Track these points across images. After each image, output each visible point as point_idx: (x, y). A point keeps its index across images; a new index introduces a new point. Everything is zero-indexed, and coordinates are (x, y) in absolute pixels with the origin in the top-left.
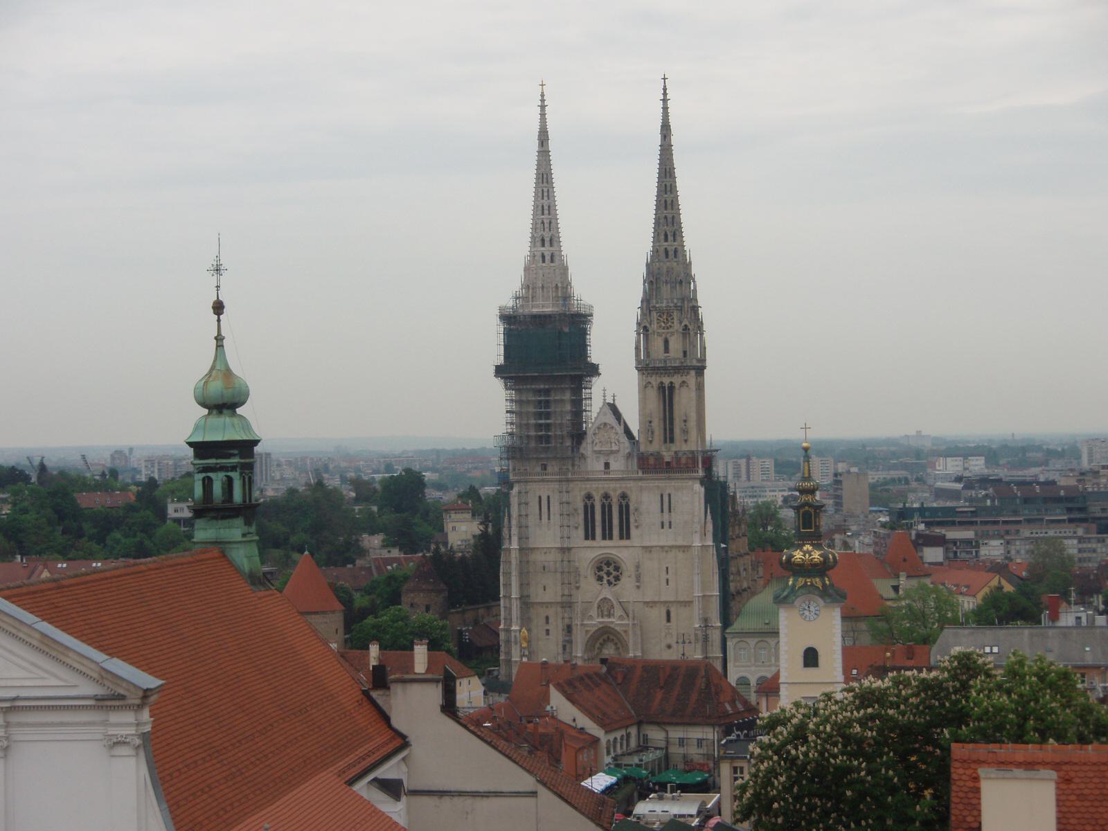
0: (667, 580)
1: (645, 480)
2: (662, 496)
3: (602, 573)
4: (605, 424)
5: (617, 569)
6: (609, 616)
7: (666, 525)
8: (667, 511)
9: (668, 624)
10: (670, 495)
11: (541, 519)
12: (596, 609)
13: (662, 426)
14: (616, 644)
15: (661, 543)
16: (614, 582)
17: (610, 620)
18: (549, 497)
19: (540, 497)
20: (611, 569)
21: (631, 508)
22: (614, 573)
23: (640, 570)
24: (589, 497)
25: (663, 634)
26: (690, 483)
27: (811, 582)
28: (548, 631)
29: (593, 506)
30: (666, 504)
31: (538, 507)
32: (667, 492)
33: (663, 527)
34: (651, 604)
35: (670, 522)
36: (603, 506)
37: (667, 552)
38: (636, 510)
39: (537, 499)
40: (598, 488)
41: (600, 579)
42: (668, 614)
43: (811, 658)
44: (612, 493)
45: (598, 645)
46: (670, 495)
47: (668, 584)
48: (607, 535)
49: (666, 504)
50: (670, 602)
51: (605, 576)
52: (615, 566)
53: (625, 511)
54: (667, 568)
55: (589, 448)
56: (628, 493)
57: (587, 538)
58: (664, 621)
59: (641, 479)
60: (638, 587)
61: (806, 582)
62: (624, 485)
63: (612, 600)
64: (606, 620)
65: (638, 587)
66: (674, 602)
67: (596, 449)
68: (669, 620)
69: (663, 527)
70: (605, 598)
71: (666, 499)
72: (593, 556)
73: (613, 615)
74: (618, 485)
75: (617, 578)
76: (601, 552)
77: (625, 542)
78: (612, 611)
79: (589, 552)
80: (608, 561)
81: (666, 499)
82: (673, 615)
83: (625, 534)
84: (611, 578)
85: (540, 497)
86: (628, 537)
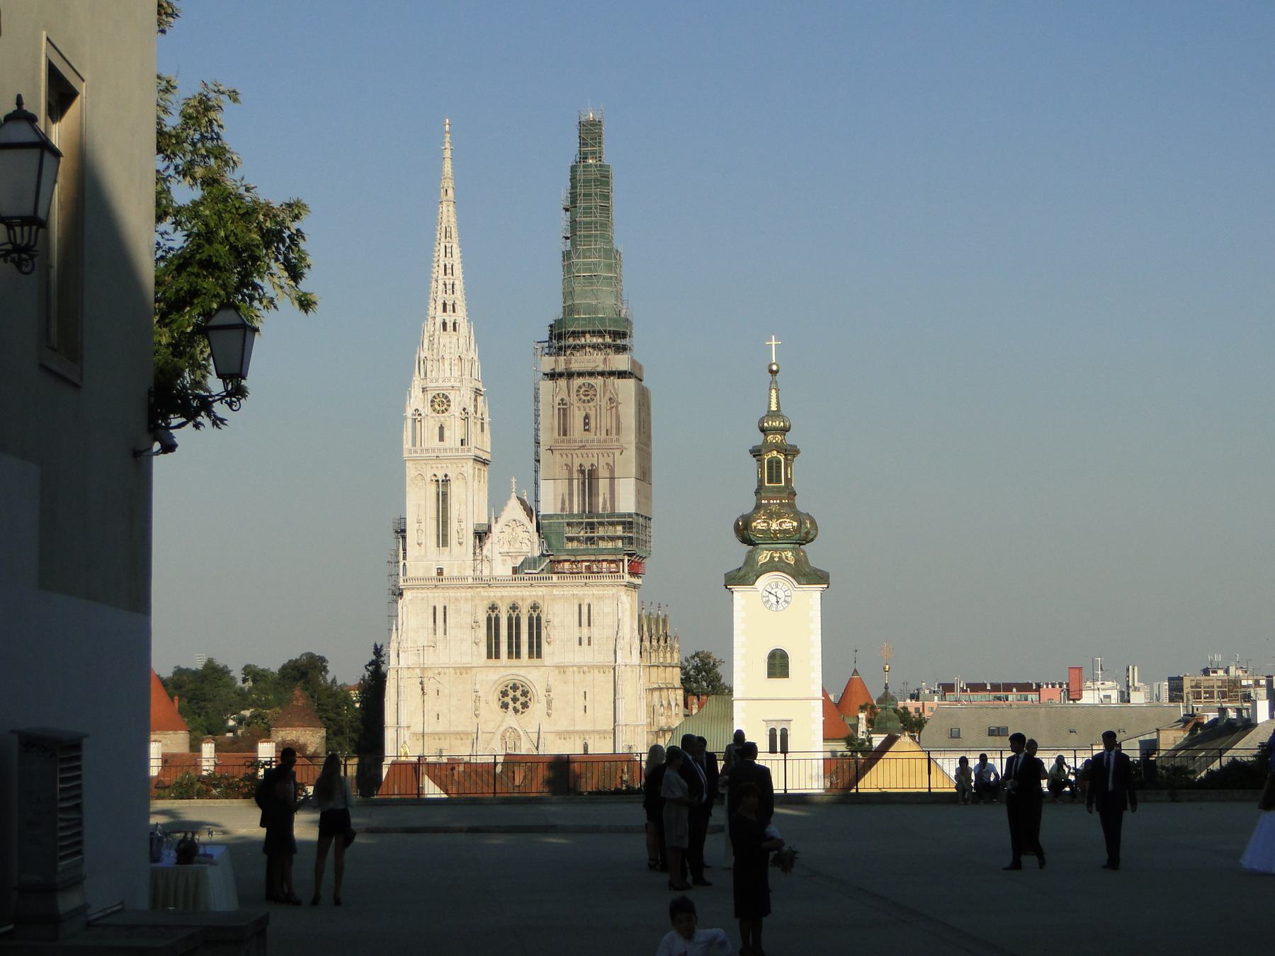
0: (585, 707)
2: (580, 606)
5: (525, 694)
7: (585, 641)
8: (587, 624)
10: (589, 605)
11: (435, 634)
16: (521, 710)
18: (445, 608)
19: (435, 608)
22: (522, 699)
24: (493, 608)
26: (614, 590)
27: (780, 558)
29: (497, 619)
30: (585, 616)
32: (586, 602)
33: (580, 644)
34: (564, 735)
35: (589, 638)
40: (502, 596)
41: (505, 706)
43: (778, 664)
44: (520, 603)
46: (589, 605)
49: (585, 616)
51: (511, 705)
53: (536, 625)
54: (585, 692)
55: (497, 548)
56: (541, 602)
57: (489, 656)
60: (549, 715)
61: (772, 557)
62: (534, 593)
66: (594, 732)
67: (501, 550)
69: (580, 644)
71: (585, 610)
72: (496, 677)
75: (525, 705)
76: (505, 674)
77: (535, 661)
78: (518, 744)
80: (515, 684)
81: (585, 610)
83: (536, 650)
84: (518, 705)
85: (435, 608)
86: (539, 655)
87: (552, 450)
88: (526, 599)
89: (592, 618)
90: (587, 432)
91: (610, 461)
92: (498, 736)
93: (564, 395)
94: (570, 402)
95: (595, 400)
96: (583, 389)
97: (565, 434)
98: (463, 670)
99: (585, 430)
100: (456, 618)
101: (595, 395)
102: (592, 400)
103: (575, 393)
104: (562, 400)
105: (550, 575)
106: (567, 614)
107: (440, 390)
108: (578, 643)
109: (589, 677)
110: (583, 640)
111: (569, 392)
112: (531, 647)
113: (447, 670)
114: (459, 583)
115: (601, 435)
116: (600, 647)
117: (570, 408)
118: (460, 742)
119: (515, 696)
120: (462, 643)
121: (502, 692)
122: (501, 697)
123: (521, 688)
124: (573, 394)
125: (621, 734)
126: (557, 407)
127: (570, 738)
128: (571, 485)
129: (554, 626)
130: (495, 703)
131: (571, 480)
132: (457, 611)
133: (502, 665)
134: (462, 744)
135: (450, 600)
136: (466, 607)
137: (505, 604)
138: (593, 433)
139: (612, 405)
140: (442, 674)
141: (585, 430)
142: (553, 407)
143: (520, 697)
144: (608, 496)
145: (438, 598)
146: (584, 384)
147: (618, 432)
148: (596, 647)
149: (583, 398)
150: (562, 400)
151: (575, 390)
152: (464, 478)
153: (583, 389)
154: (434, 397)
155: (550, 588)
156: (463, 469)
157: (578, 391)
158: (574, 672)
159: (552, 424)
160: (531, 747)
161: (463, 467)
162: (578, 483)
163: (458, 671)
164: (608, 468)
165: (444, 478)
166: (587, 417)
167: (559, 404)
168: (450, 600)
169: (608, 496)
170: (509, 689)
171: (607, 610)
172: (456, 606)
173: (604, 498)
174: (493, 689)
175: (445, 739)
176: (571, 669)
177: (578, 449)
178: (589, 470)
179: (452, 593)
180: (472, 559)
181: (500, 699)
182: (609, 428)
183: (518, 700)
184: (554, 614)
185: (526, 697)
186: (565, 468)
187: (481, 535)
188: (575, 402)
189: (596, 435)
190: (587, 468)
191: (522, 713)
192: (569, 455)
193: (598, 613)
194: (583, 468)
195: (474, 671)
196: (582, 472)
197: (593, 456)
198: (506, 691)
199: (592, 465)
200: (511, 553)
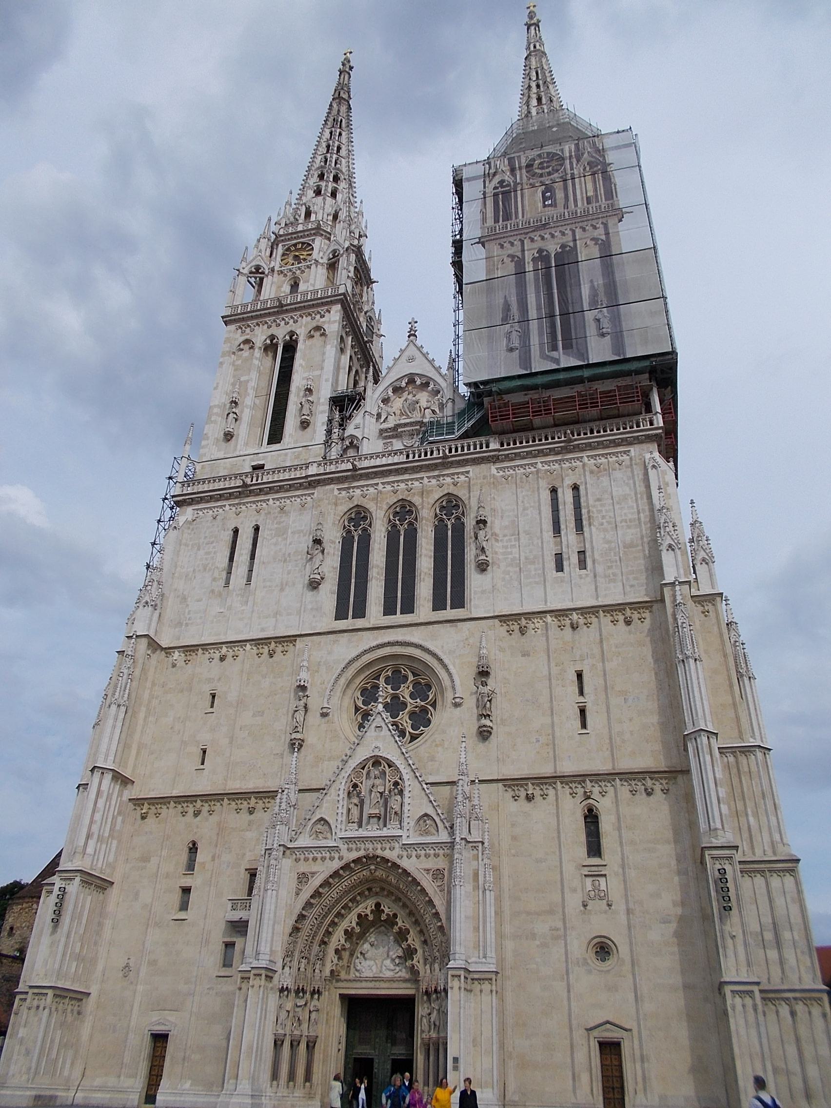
0: (583, 711)
1: (508, 458)
2: (554, 491)
4: (411, 380)
5: (422, 689)
6: (382, 819)
8: (572, 524)
9: (595, 861)
10: (576, 488)
12: (343, 795)
14: (402, 936)
17: (385, 832)
18: (257, 529)
19: (236, 531)
20: (405, 692)
21: (469, 522)
23: (490, 681)
26: (634, 450)
28: (186, 891)
31: (227, 554)
32: (568, 482)
33: (560, 567)
35: (582, 553)
37: (574, 627)
38: (482, 523)
39: (228, 535)
42: (591, 818)
44: (416, 500)
45: (338, 938)
46: (576, 488)
47: (584, 725)
50: (596, 777)
52: (416, 684)
54: (580, 675)
56: (462, 493)
57: (341, 614)
58: (582, 850)
59: (495, 459)
63: (399, 762)
64: (372, 830)
65: (484, 734)
66: (610, 776)
67: (385, 426)
68: (594, 848)
69: (560, 567)
70: (377, 761)
71: (566, 497)
73: (399, 815)
75: (421, 719)
76: (374, 644)
77: (449, 613)
81: (566, 497)
82: (606, 825)
84: (404, 719)
85: (236, 531)
86: (459, 602)
88: (430, 492)
89: (584, 511)
91: (600, 233)
92: (342, 785)
100: (276, 544)
102: (557, 171)
104: (502, 182)
105: (483, 439)
106: (524, 509)
107: (298, 238)
108: (551, 564)
109: (588, 636)
110: (565, 556)
111: (513, 170)
115: (576, 205)
116: (610, 567)
117: (515, 191)
118: (245, 816)
119: (395, 697)
120: (282, 590)
121: (364, 691)
122: (360, 704)
123: (411, 678)
125: (708, 758)
127: (544, 796)
128: (521, 286)
129: (494, 534)
130: (345, 716)
131: (520, 272)
134: (250, 823)
137: (385, 507)
138: (560, 209)
139: (595, 169)
140: (229, 659)
141: (545, 206)
142: (484, 194)
143: (409, 700)
144: (600, 281)
146: (539, 156)
148: (600, 569)
149: (540, 171)
151: (524, 164)
152: (323, 335)
154: (288, 249)
156: (322, 320)
157: (528, 166)
160: (430, 811)
161: (322, 316)
164: (596, 244)
165: (288, 338)
167: (495, 188)
169: (601, 282)
170: (382, 682)
171: (617, 491)
172: (279, 523)
173: (592, 288)
174: (343, 681)
175: (210, 812)
176: (538, 623)
177: (534, 231)
179: (272, 502)
182: (590, 194)
184: (494, 510)
185: (425, 698)
186: (507, 260)
188: (525, 178)
189: (566, 206)
190: (553, 247)
191: (413, 738)
192: (517, 243)
193: (599, 500)
194: (545, 253)
196: (542, 256)
197: (563, 234)
200: (405, 425)
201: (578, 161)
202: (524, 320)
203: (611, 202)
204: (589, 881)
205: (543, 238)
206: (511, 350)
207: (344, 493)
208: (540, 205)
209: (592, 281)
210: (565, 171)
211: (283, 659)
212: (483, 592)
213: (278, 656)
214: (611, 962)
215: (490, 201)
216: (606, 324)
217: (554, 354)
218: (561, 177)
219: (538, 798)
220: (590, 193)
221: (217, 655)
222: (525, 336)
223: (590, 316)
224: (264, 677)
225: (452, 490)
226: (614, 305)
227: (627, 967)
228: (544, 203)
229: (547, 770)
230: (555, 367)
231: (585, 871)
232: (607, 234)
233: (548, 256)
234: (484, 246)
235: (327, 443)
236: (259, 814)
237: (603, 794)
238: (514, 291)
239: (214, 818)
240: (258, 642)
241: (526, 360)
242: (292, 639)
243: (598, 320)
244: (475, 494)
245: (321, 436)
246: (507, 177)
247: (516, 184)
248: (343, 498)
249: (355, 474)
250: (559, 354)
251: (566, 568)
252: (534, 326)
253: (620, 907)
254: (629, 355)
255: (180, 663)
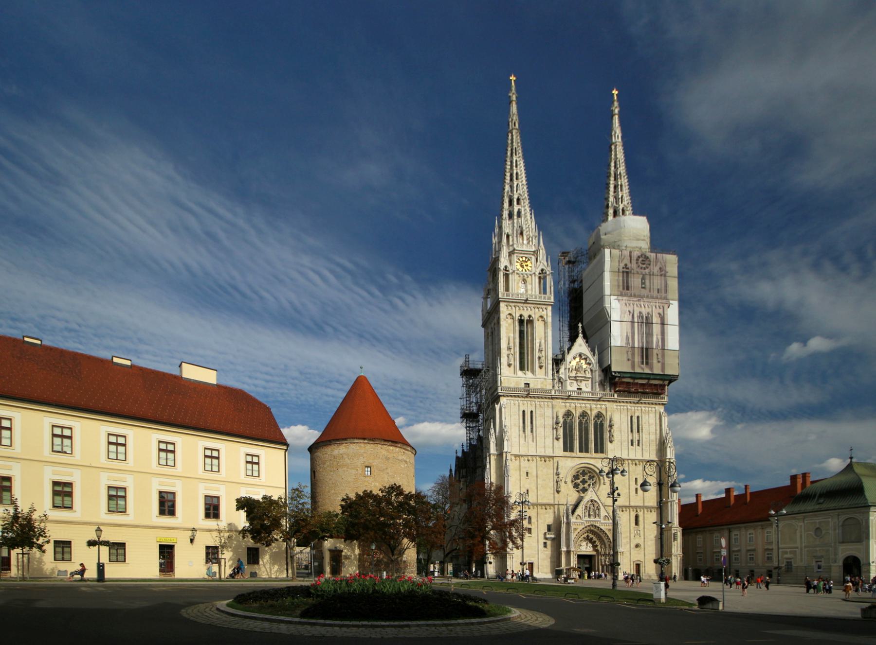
3: (578, 481)
9: (636, 527)
11: (524, 431)
13: (640, 354)
15: (632, 457)
18: (532, 412)
19: (524, 412)
21: (606, 424)
24: (568, 414)
25: (632, 535)
36: (580, 423)
37: (636, 464)
42: (637, 517)
44: (589, 412)
48: (584, 448)
50: (640, 507)
53: (599, 428)
54: (636, 479)
57: (565, 450)
68: (637, 523)
74: (594, 406)
76: (580, 463)
79: (570, 464)
82: (641, 519)
83: (600, 448)
85: (524, 412)
87: (619, 300)
90: (643, 290)
91: (661, 311)
93: (627, 261)
94: (631, 268)
95: (649, 268)
96: (641, 259)
97: (628, 289)
98: (545, 458)
99: (642, 288)
101: (650, 265)
102: (648, 268)
103: (635, 262)
104: (626, 265)
112: (596, 445)
113: (534, 458)
114: (545, 396)
117: (631, 272)
124: (634, 262)
126: (621, 270)
127: (626, 511)
128: (633, 327)
131: (633, 322)
132: (543, 415)
133: (577, 456)
135: (536, 407)
136: (548, 412)
140: (531, 461)
144: (660, 337)
145: (527, 405)
147: (666, 291)
149: (641, 265)
150: (626, 265)
151: (635, 259)
153: (641, 259)
155: (611, 403)
157: (637, 260)
158: (629, 464)
159: (618, 280)
162: (638, 325)
163: (543, 459)
164: (660, 317)
166: (643, 279)
167: (623, 268)
168: (536, 407)
172: (540, 411)
173: (657, 338)
178: (646, 317)
180: (552, 378)
181: (572, 481)
183: (586, 482)
186: (628, 313)
187: (558, 362)
189: (650, 291)
195: (556, 459)
198: (578, 475)
199: (648, 313)
201: (656, 265)
202: (633, 347)
203: (665, 295)
204: (636, 531)
205: (641, 306)
206: (628, 360)
207: (563, 404)
208: (640, 286)
209: (657, 335)
210: (650, 269)
211: (550, 463)
212: (611, 450)
213: (547, 462)
214: (638, 549)
215: (621, 274)
216: (660, 356)
217: (642, 366)
218: (649, 273)
219: (625, 511)
220: (659, 287)
221: (526, 459)
222: (633, 354)
223: (655, 352)
224: (544, 468)
225: (600, 410)
226: (663, 349)
227: (643, 550)
228: (642, 285)
229: (627, 504)
230: (642, 371)
231: (635, 529)
232: (664, 313)
233: (642, 317)
234: (619, 302)
235: (553, 379)
236: (548, 510)
237: (640, 511)
238: (630, 331)
239: (535, 510)
240: (541, 457)
241: (633, 366)
242: (553, 457)
243: (657, 355)
244: (609, 414)
245: (551, 377)
246: (629, 265)
247: (632, 269)
248: (563, 406)
249: (569, 398)
250: (644, 366)
251: (634, 445)
252: (636, 351)
253: (642, 537)
254: (666, 373)
255: (514, 460)
